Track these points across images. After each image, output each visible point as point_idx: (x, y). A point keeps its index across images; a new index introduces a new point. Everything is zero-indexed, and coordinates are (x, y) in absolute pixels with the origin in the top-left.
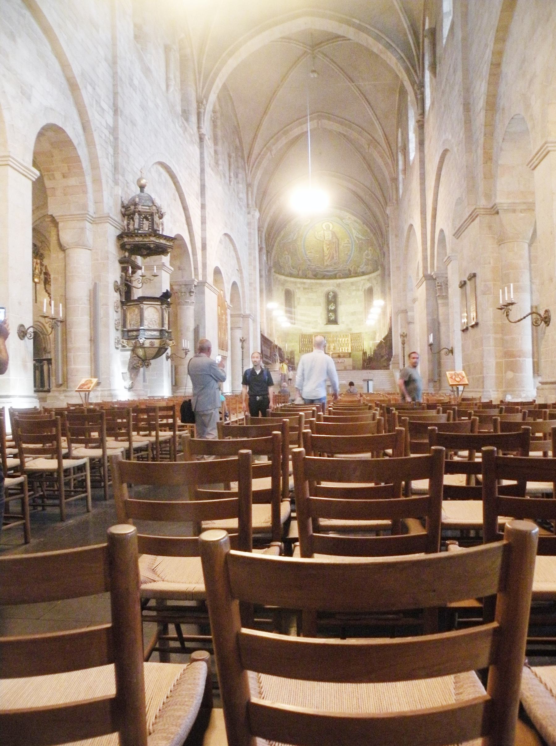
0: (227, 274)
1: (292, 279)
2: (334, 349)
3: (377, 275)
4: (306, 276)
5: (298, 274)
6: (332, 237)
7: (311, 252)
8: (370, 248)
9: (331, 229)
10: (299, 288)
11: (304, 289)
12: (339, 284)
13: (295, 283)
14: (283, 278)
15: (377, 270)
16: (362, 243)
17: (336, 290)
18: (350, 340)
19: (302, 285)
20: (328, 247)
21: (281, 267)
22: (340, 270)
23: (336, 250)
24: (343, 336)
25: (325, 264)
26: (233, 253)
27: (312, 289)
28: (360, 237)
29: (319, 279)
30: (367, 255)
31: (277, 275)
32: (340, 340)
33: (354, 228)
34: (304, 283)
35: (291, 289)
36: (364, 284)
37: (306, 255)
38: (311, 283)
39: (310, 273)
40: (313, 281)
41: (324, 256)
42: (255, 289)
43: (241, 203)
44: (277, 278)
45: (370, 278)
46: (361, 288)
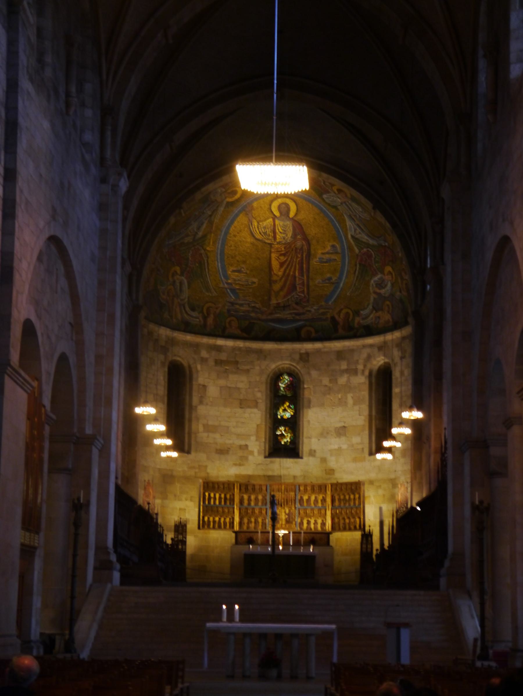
0: (49, 337)
1: (189, 338)
2: (288, 521)
6: (294, 235)
8: (388, 269)
9: (292, 214)
10: (204, 361)
11: (218, 362)
12: (307, 354)
13: (197, 347)
14: (164, 332)
15: (406, 323)
17: (299, 368)
18: (329, 500)
19: (214, 353)
20: (283, 259)
24: (313, 487)
25: (274, 302)
26: (63, 282)
27: (237, 363)
28: (364, 238)
29: (256, 338)
30: (380, 285)
31: (152, 326)
32: (305, 497)
33: (350, 217)
34: (219, 349)
35: (185, 364)
37: (226, 277)
38: (234, 349)
40: (240, 344)
41: (271, 282)
42: (110, 370)
43: (87, 157)
44: (150, 333)
45: (385, 343)
46: (360, 367)
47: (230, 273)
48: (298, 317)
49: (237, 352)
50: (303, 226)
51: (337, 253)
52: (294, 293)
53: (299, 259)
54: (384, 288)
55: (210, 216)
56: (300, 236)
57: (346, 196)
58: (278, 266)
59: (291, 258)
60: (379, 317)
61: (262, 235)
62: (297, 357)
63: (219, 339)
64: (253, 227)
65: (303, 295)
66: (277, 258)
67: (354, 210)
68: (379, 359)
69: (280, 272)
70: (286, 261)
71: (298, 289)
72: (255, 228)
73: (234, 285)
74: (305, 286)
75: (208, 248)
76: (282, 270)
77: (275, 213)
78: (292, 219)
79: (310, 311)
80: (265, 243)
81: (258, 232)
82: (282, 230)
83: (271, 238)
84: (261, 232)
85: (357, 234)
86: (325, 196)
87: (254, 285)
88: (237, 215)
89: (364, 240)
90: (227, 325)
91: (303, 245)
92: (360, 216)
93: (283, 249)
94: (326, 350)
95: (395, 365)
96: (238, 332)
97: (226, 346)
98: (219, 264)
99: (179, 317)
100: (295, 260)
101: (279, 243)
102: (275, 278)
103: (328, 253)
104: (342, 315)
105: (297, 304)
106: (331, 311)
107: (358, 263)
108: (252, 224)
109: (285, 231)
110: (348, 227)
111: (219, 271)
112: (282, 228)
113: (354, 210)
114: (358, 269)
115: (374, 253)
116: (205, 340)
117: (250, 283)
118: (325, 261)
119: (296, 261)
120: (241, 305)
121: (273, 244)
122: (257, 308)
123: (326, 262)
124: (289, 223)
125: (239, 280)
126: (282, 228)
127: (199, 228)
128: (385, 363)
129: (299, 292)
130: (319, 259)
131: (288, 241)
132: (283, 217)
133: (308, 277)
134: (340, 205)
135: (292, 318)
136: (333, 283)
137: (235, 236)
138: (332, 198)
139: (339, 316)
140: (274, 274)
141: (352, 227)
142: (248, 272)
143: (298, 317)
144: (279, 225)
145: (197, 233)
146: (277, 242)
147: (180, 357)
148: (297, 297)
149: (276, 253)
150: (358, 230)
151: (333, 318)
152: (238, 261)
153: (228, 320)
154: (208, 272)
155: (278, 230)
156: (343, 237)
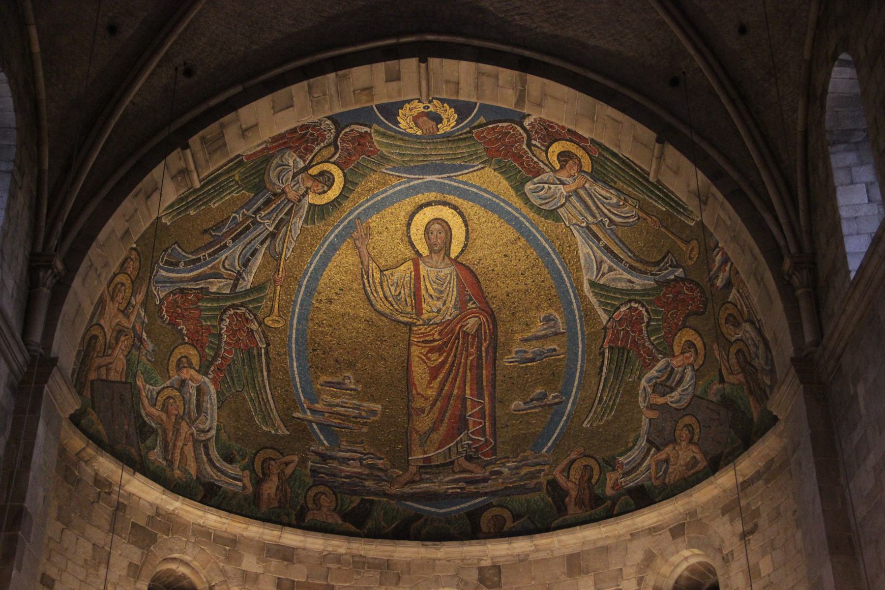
3: (744, 486)
4: (302, 512)
5: (256, 497)
6: (462, 304)
7: (339, 386)
9: (455, 250)
12: (497, 569)
16: (633, 321)
19: (274, 562)
20: (436, 359)
21: (144, 431)
22: (507, 491)
23: (478, 380)
25: (417, 456)
30: (663, 387)
34: (287, 555)
36: (649, 558)
37: (313, 398)
38: (324, 557)
39: (327, 501)
40: (338, 545)
44: (102, 484)
45: (692, 514)
47: (319, 386)
48: (472, 488)
49: (329, 565)
50: (481, 279)
51: (556, 334)
52: (462, 436)
53: (471, 358)
54: (673, 390)
55: (273, 235)
56: (474, 303)
57: (581, 170)
58: (427, 377)
59: (455, 356)
60: (667, 461)
61: (390, 302)
62: (474, 575)
63: (286, 528)
64: (371, 280)
65: (483, 439)
66: (424, 358)
67: (598, 207)
68: (675, 559)
69: (432, 388)
70: (443, 363)
71: (471, 426)
72: (374, 282)
73: (327, 415)
74: (487, 419)
75: (268, 322)
76: (436, 384)
77: (418, 247)
78: (455, 261)
79: (499, 473)
80: (399, 322)
81: (381, 293)
82: (433, 288)
83: (409, 309)
84: (388, 294)
85: (603, 274)
86: (529, 186)
87: (373, 419)
88: (333, 248)
89: (620, 285)
90: (310, 506)
91: (481, 324)
92: (611, 221)
93: (436, 337)
94: (542, 555)
95: (726, 560)
96: (335, 520)
97: (304, 549)
98: (295, 364)
99: (193, 472)
100: (463, 361)
101: (427, 323)
102: (418, 403)
103: (537, 338)
104: (575, 475)
105: (469, 458)
106: (546, 467)
107: (606, 346)
108: (367, 273)
109: (441, 292)
110: (582, 261)
111: (294, 378)
112: (435, 286)
113: (598, 207)
114: (606, 362)
115: (647, 311)
116: (254, 530)
117: (363, 414)
118: (530, 356)
119: (466, 363)
120: (344, 461)
121: (415, 324)
122: (380, 469)
123: (532, 360)
124: (447, 271)
125: (338, 405)
126: (435, 286)
127: (245, 265)
128: (692, 569)
129: (471, 433)
130: (517, 352)
131: (448, 318)
132: (435, 257)
133: (493, 398)
134: (562, 206)
135: (459, 490)
136: (550, 406)
137: (330, 301)
138: (546, 186)
139: (568, 477)
140: (418, 394)
141: (593, 257)
142: (360, 387)
143: (472, 488)
144: (427, 280)
145: (239, 274)
146: (423, 320)
147: (187, 564)
148: (468, 444)
149: (420, 344)
150: (608, 262)
151: (553, 484)
152: (337, 361)
153: (311, 493)
154: (269, 380)
155: (427, 290)
156: (571, 291)
